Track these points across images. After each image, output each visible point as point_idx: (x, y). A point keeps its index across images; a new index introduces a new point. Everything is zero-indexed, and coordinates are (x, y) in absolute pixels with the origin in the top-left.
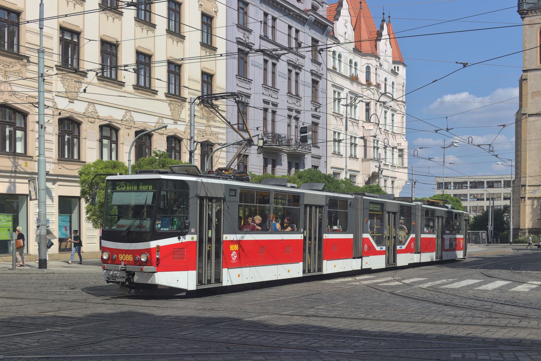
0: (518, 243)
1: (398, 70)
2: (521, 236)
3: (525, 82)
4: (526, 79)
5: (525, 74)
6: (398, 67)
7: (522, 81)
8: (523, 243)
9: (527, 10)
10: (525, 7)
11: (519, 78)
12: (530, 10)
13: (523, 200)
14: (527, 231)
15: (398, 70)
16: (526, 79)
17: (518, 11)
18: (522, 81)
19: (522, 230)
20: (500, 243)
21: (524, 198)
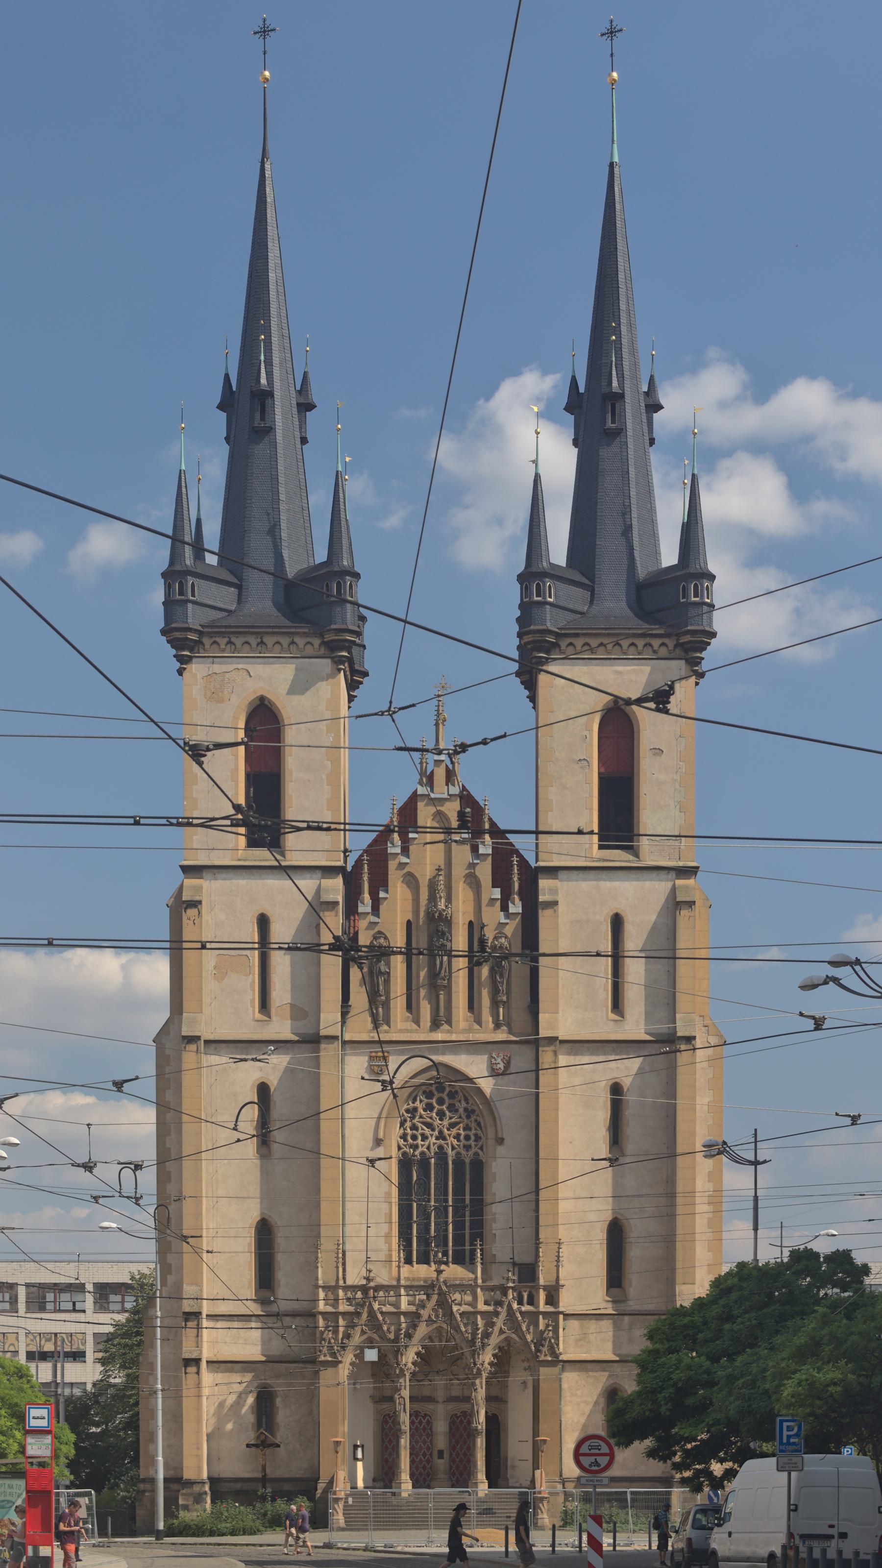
0: (180, 1534)
2: (186, 1508)
3: (192, 912)
4: (195, 904)
5: (190, 882)
7: (182, 906)
8: (202, 1535)
9: (200, 633)
10: (194, 617)
11: (167, 896)
12: (210, 635)
13: (192, 1369)
14: (207, 1488)
16: (195, 904)
17: (164, 632)
18: (182, 906)
19: (190, 1483)
20: (114, 1535)
21: (197, 1361)
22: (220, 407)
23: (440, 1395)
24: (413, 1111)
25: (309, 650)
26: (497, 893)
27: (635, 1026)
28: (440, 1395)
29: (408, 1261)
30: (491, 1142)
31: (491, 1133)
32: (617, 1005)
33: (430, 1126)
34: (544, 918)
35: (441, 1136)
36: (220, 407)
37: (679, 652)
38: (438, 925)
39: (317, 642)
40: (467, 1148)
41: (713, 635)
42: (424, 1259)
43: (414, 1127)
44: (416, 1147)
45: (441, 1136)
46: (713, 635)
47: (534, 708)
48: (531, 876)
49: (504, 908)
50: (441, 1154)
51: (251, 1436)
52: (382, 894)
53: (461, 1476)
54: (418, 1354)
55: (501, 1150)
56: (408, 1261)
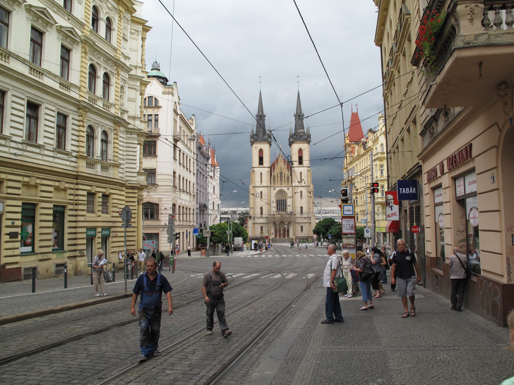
38: (281, 173)
53: (284, 236)
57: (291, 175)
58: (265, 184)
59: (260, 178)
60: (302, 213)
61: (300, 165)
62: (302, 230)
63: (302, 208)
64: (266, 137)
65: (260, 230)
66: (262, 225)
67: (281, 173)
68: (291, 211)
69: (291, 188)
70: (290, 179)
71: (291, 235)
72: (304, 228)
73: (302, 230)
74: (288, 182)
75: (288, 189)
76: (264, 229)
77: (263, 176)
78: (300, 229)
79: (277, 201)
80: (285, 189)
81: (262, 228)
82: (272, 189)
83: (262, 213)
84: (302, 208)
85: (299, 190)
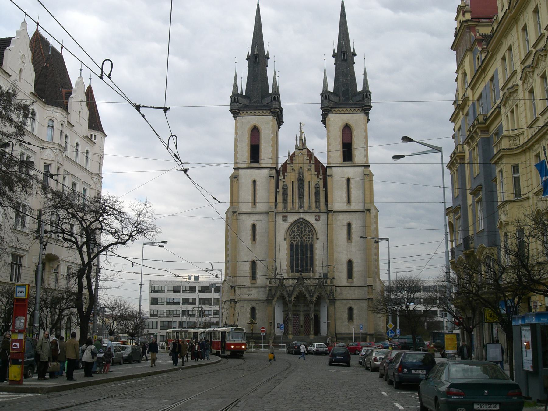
1: (95, 139)
6: (95, 136)
15: (95, 139)
22: (247, 59)
23: (302, 309)
24: (294, 231)
25: (267, 114)
26: (316, 173)
27: (356, 206)
28: (302, 309)
29: (292, 272)
30: (315, 239)
31: (315, 236)
32: (349, 201)
33: (298, 235)
34: (329, 179)
35: (302, 238)
36: (247, 59)
37: (363, 112)
38: (301, 181)
39: (269, 112)
40: (309, 241)
41: (372, 107)
42: (297, 271)
43: (294, 235)
44: (294, 241)
45: (302, 238)
46: (372, 107)
47: (325, 127)
48: (325, 169)
49: (318, 177)
50: (302, 243)
51: (248, 321)
52: (286, 174)
53: (307, 333)
54: (295, 298)
55: (317, 241)
56: (292, 272)
57: (325, 185)
58: (261, 207)
59: (251, 192)
60: (350, 275)
61: (347, 163)
62: (351, 318)
63: (350, 262)
64: (267, 100)
65: (249, 315)
66: (253, 304)
67: (301, 181)
68: (325, 271)
69: (323, 217)
70: (322, 194)
71: (324, 331)
72: (355, 311)
73: (351, 318)
74: (317, 201)
75: (318, 219)
76: (258, 315)
77: (257, 188)
78: (346, 316)
79: (291, 246)
80: (310, 218)
81: (253, 310)
82: (279, 218)
83: (254, 276)
84: (350, 262)
85: (343, 219)
